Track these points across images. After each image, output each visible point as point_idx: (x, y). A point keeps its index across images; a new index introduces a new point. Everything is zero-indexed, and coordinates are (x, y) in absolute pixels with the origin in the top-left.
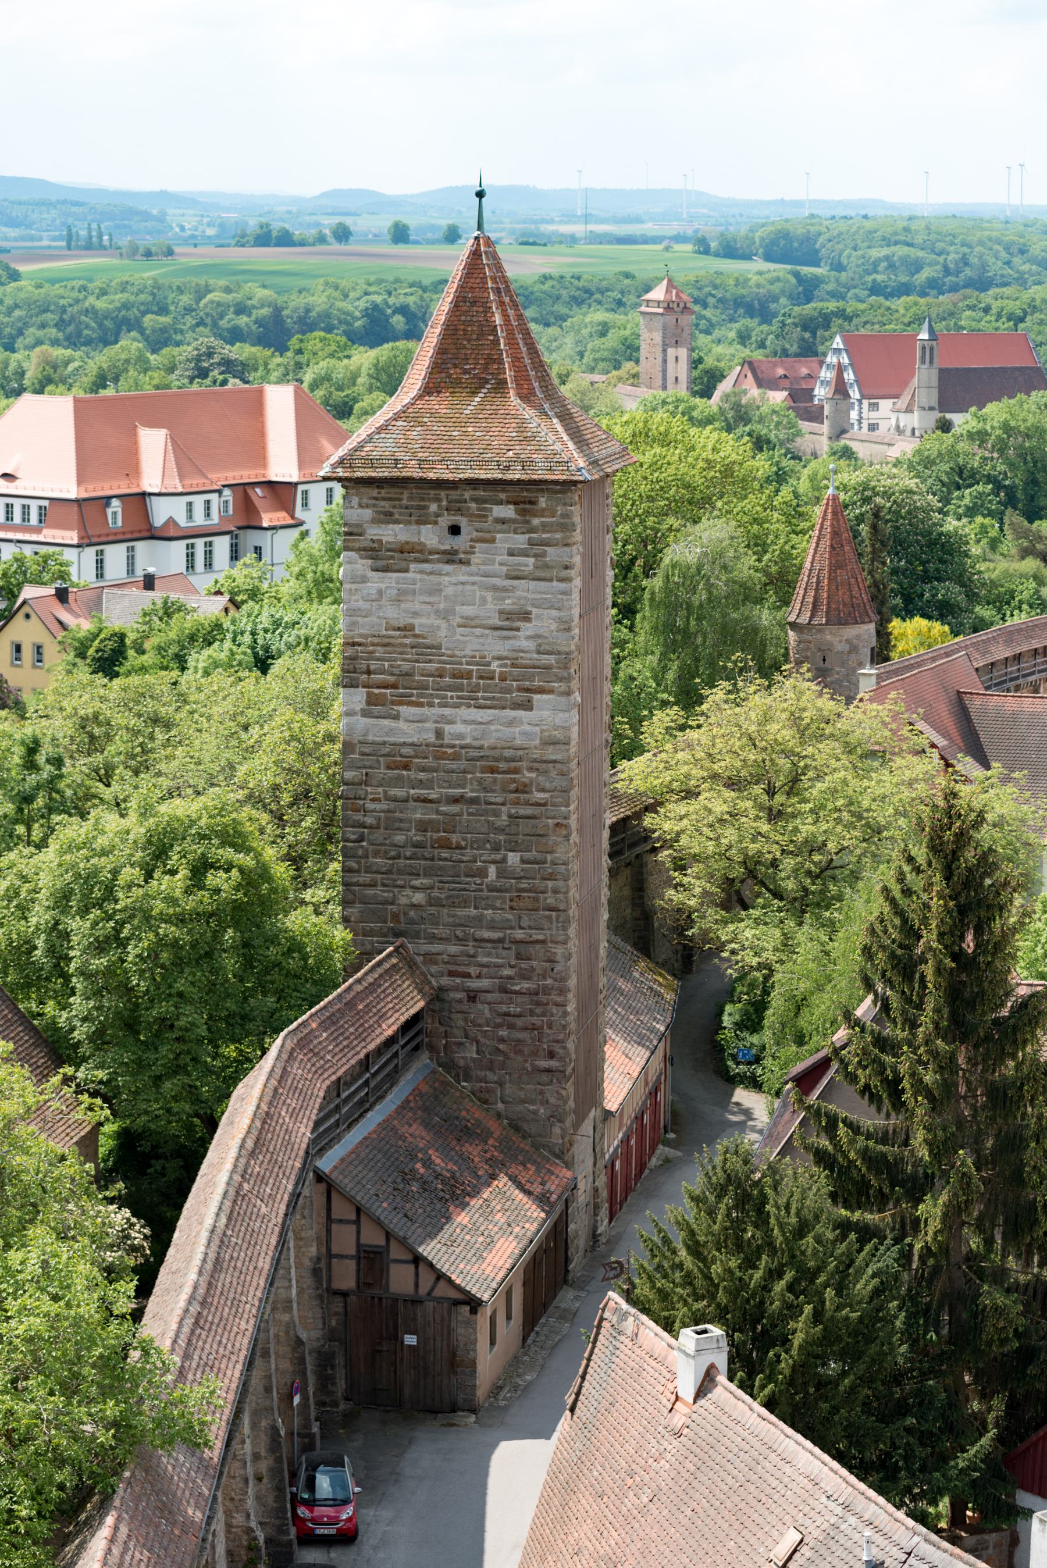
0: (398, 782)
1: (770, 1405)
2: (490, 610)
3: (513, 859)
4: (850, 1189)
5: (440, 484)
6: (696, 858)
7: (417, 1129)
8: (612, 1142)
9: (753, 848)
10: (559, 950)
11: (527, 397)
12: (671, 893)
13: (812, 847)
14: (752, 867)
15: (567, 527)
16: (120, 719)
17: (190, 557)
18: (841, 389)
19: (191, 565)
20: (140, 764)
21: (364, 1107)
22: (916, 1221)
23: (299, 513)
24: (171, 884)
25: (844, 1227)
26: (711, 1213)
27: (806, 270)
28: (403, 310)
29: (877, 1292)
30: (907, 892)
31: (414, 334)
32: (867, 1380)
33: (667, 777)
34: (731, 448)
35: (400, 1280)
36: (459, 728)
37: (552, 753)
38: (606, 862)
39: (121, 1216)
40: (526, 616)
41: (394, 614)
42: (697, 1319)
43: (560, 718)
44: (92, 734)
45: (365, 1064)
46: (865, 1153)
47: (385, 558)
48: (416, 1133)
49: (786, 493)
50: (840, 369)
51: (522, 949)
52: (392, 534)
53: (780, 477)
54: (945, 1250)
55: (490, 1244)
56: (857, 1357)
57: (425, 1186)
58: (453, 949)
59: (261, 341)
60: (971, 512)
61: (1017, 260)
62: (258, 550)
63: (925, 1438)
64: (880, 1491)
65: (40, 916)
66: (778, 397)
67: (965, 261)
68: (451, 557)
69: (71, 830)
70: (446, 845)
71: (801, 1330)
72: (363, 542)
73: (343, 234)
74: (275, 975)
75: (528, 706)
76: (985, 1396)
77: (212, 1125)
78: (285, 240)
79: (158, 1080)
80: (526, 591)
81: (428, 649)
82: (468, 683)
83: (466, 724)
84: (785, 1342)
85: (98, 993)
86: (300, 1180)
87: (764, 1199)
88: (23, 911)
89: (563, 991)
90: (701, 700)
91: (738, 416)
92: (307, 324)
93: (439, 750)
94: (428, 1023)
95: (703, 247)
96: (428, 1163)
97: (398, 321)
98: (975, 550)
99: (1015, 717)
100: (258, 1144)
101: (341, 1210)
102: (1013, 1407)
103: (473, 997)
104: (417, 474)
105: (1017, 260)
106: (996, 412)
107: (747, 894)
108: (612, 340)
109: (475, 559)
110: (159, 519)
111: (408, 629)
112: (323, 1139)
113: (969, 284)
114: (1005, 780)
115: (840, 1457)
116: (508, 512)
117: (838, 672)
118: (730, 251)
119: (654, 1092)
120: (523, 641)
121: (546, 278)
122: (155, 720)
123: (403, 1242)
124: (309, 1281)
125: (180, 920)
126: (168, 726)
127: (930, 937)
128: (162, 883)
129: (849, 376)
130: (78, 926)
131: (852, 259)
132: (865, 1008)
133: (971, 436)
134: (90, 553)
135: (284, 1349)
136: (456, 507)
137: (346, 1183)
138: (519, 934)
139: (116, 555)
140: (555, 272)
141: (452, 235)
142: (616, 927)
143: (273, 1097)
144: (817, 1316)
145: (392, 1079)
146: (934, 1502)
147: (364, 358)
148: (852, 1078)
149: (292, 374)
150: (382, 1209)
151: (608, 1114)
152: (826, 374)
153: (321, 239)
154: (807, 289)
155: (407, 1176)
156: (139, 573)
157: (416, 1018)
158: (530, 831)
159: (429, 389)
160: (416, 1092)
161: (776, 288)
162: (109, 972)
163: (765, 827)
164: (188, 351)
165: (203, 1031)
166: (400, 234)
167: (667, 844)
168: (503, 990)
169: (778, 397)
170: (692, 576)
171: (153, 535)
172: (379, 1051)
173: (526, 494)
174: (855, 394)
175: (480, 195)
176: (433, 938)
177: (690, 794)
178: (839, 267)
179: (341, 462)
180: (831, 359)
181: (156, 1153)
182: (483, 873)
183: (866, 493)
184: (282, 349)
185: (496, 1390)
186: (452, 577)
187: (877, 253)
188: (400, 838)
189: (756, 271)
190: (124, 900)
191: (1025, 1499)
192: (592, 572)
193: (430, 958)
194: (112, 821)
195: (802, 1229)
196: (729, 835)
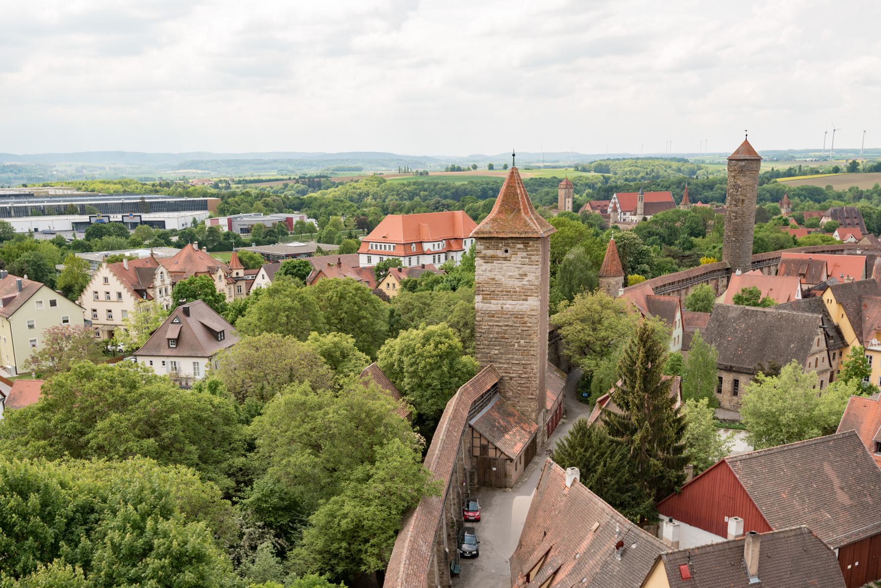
0: (491, 321)
1: (591, 488)
2: (516, 273)
3: (522, 342)
4: (615, 432)
5: (502, 239)
6: (572, 341)
8: (548, 418)
9: (588, 339)
11: (527, 213)
12: (565, 351)
13: (604, 339)
14: (588, 344)
16: (416, 304)
17: (434, 259)
18: (615, 210)
19: (434, 261)
20: (421, 316)
21: (482, 407)
22: (632, 441)
23: (464, 247)
24: (430, 347)
25: (612, 442)
26: (576, 438)
27: (606, 175)
28: (492, 189)
29: (621, 460)
30: (632, 351)
31: (495, 196)
32: (617, 483)
33: (564, 319)
34: (583, 227)
35: (492, 453)
36: (507, 306)
38: (548, 342)
39: (418, 436)
40: (526, 275)
41: (489, 274)
42: (571, 465)
44: (408, 308)
45: (482, 396)
46: (618, 422)
47: (488, 259)
48: (496, 415)
49: (598, 239)
50: (615, 204)
51: (525, 366)
52: (490, 252)
53: (597, 235)
54: (640, 448)
55: (516, 444)
56: (615, 476)
58: (506, 366)
59: (453, 199)
60: (652, 244)
61: (668, 170)
63: (633, 499)
64: (621, 513)
65: (396, 356)
66: (597, 212)
67: (653, 171)
68: (505, 259)
69: (403, 333)
71: (600, 468)
72: (481, 255)
73: (475, 167)
74: (459, 373)
75: (526, 300)
76: (650, 488)
77: (441, 411)
78: (459, 169)
79: (427, 400)
80: (526, 268)
82: (510, 294)
83: (510, 305)
84: (595, 472)
85: (411, 378)
86: (465, 427)
87: (590, 434)
88: (391, 355)
90: (573, 298)
91: (585, 218)
92: (465, 193)
93: (502, 312)
95: (576, 168)
96: (499, 423)
97: (491, 192)
98: (653, 255)
99: (663, 302)
100: (454, 417)
101: (475, 435)
102: (659, 491)
103: (511, 378)
104: (496, 236)
105: (668, 170)
106: (660, 214)
107: (586, 351)
108: (549, 197)
111: (493, 279)
112: (471, 416)
113: (653, 177)
114: (660, 320)
115: (610, 503)
116: (521, 246)
117: (613, 290)
118: (584, 170)
119: (560, 405)
121: (532, 179)
122: (425, 304)
123: (492, 444)
124: (467, 453)
125: (432, 357)
126: (429, 305)
127: (638, 363)
128: (427, 347)
129: (618, 206)
130: (404, 359)
131: (619, 171)
132: (619, 383)
133: (653, 221)
134: (407, 259)
136: (507, 245)
137: (477, 428)
138: (524, 362)
139: (414, 259)
140: (534, 177)
141: (505, 167)
142: (550, 360)
143: (458, 404)
144: (605, 466)
145: (489, 400)
146: (636, 516)
147: (481, 203)
148: (615, 402)
149: (461, 208)
150: (487, 435)
151: (547, 411)
152: (611, 205)
153: (469, 169)
154: (607, 180)
155: (494, 426)
156: (420, 264)
157: (496, 384)
159: (500, 212)
161: (596, 181)
162: (414, 372)
163: (591, 333)
164: (433, 201)
165: (439, 387)
166: (491, 167)
167: (564, 338)
169: (597, 212)
170: (570, 262)
172: (486, 393)
173: (526, 241)
174: (619, 211)
175: (514, 155)
176: (500, 363)
177: (570, 324)
178: (615, 174)
179: (475, 233)
180: (613, 200)
181: (427, 419)
182: (514, 345)
183: (622, 238)
184: (459, 201)
185: (517, 483)
187: (627, 169)
188: (491, 336)
189: (591, 174)
190: (417, 352)
191: (661, 517)
192: (544, 263)
193: (500, 368)
194: (415, 332)
195: (601, 442)
196: (581, 335)
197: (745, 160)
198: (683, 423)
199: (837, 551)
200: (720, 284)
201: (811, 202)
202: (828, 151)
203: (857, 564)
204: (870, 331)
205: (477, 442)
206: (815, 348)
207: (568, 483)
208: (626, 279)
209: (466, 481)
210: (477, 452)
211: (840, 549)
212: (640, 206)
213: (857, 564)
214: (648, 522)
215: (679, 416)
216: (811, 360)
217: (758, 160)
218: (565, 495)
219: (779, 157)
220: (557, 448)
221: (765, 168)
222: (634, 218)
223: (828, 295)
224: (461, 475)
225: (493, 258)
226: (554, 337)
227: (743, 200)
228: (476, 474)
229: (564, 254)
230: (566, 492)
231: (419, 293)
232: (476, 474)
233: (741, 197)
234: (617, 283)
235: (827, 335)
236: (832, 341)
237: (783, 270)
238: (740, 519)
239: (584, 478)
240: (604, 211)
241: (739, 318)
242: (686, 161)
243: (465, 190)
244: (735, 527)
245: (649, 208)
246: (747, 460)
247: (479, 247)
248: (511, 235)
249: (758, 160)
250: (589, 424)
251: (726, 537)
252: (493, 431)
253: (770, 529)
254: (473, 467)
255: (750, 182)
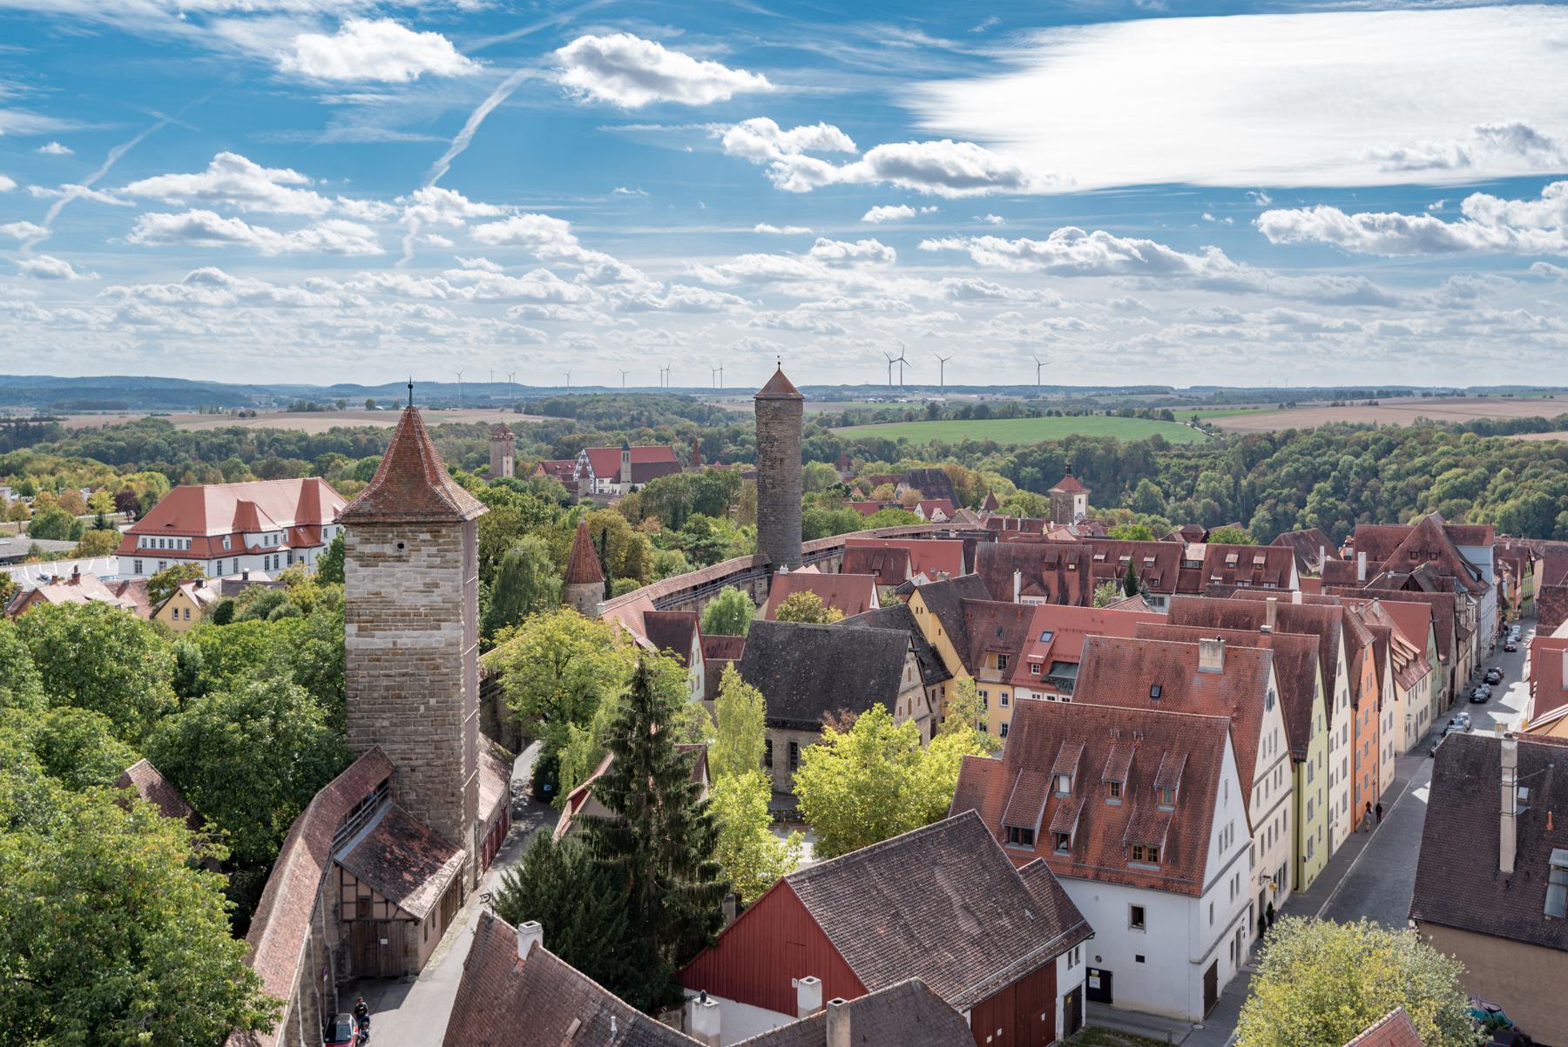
0: (375, 667)
3: (433, 701)
5: (393, 524)
7: (386, 836)
8: (484, 836)
10: (456, 744)
15: (456, 543)
18: (584, 475)
23: (323, 540)
35: (379, 911)
36: (405, 640)
37: (450, 650)
38: (478, 700)
40: (437, 586)
41: (372, 587)
43: (455, 633)
45: (358, 807)
47: (366, 561)
50: (585, 465)
51: (437, 745)
52: (369, 549)
57: (391, 864)
58: (404, 747)
62: (302, 558)
68: (399, 559)
70: (399, 697)
72: (355, 553)
75: (438, 628)
80: (436, 574)
81: (387, 603)
82: (408, 618)
83: (409, 638)
89: (459, 763)
93: (395, 652)
94: (392, 784)
96: (392, 853)
106: (658, 481)
109: (412, 559)
110: (250, 546)
116: (427, 536)
120: (436, 598)
124: (332, 917)
129: (589, 468)
135: (319, 953)
138: (436, 737)
145: (374, 811)
151: (481, 822)
152: (578, 467)
157: (385, 782)
158: (442, 687)
160: (386, 818)
168: (428, 765)
171: (247, 553)
180: (581, 460)
182: (418, 709)
184: (312, 461)
186: (399, 569)
188: (376, 695)
191: (688, 992)
192: (468, 563)
193: (392, 752)
197: (779, 398)
198: (714, 825)
199: (968, 1015)
200: (758, 590)
201: (880, 463)
202: (896, 388)
203: (999, 1032)
204: (980, 652)
205: (350, 894)
206: (904, 684)
207: (523, 953)
208: (608, 586)
209: (329, 973)
210: (350, 912)
211: (975, 1011)
212: (626, 470)
213: (999, 1032)
214: (667, 1000)
215: (706, 814)
216: (901, 702)
217: (800, 400)
218: (517, 975)
219: (831, 394)
220: (502, 887)
221: (810, 410)
222: (617, 487)
223: (916, 601)
224: (320, 960)
225: (378, 557)
226: (490, 688)
227: (782, 460)
228: (348, 955)
229: (498, 551)
230: (518, 969)
231: (235, 625)
232: (348, 955)
233: (779, 456)
234: (595, 594)
235: (921, 664)
236: (928, 672)
237: (848, 566)
238: (816, 980)
239: (551, 940)
240: (567, 478)
241: (789, 642)
242: (693, 400)
243: (325, 442)
244: (809, 993)
245: (640, 472)
246: (812, 876)
247: (351, 539)
248: (408, 519)
249: (800, 400)
250: (556, 839)
251: (793, 1012)
252: (382, 870)
253: (866, 992)
254: (343, 944)
255: (790, 433)
